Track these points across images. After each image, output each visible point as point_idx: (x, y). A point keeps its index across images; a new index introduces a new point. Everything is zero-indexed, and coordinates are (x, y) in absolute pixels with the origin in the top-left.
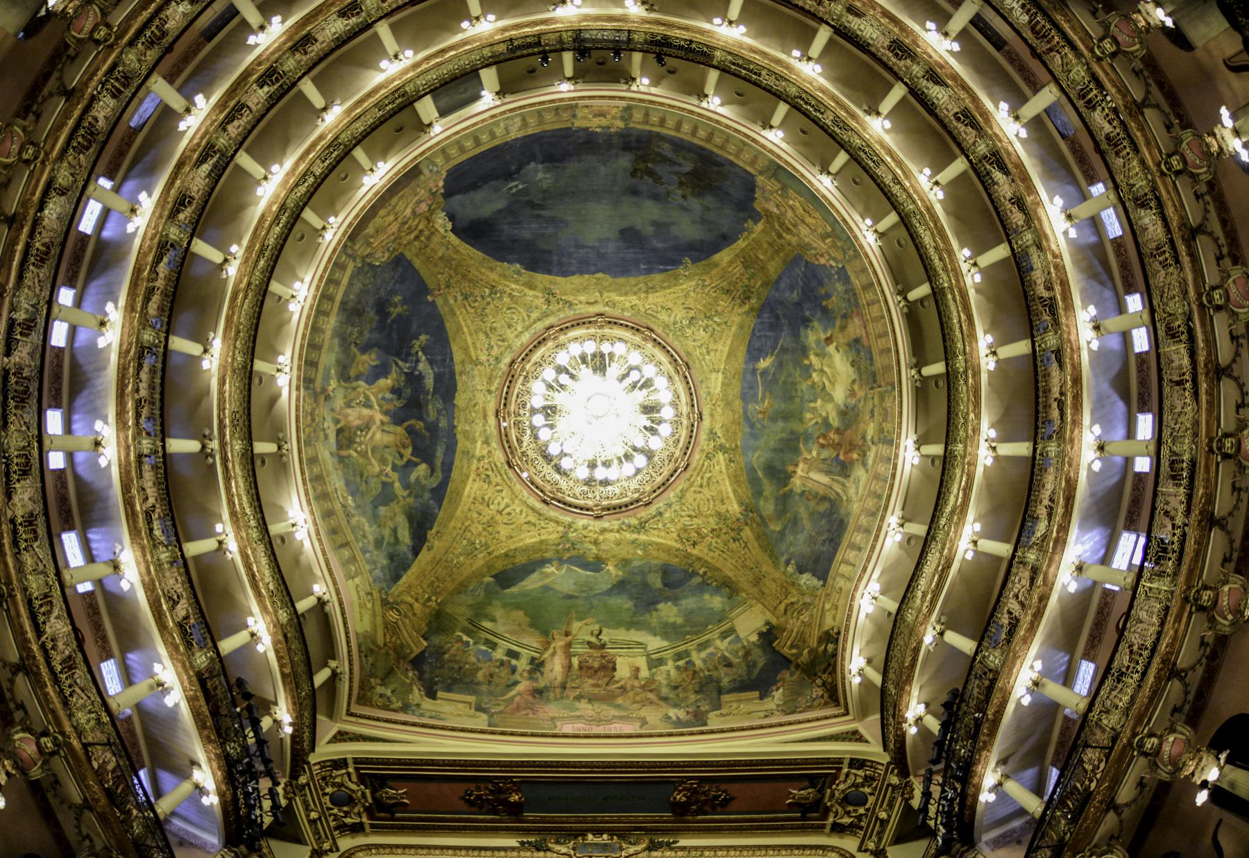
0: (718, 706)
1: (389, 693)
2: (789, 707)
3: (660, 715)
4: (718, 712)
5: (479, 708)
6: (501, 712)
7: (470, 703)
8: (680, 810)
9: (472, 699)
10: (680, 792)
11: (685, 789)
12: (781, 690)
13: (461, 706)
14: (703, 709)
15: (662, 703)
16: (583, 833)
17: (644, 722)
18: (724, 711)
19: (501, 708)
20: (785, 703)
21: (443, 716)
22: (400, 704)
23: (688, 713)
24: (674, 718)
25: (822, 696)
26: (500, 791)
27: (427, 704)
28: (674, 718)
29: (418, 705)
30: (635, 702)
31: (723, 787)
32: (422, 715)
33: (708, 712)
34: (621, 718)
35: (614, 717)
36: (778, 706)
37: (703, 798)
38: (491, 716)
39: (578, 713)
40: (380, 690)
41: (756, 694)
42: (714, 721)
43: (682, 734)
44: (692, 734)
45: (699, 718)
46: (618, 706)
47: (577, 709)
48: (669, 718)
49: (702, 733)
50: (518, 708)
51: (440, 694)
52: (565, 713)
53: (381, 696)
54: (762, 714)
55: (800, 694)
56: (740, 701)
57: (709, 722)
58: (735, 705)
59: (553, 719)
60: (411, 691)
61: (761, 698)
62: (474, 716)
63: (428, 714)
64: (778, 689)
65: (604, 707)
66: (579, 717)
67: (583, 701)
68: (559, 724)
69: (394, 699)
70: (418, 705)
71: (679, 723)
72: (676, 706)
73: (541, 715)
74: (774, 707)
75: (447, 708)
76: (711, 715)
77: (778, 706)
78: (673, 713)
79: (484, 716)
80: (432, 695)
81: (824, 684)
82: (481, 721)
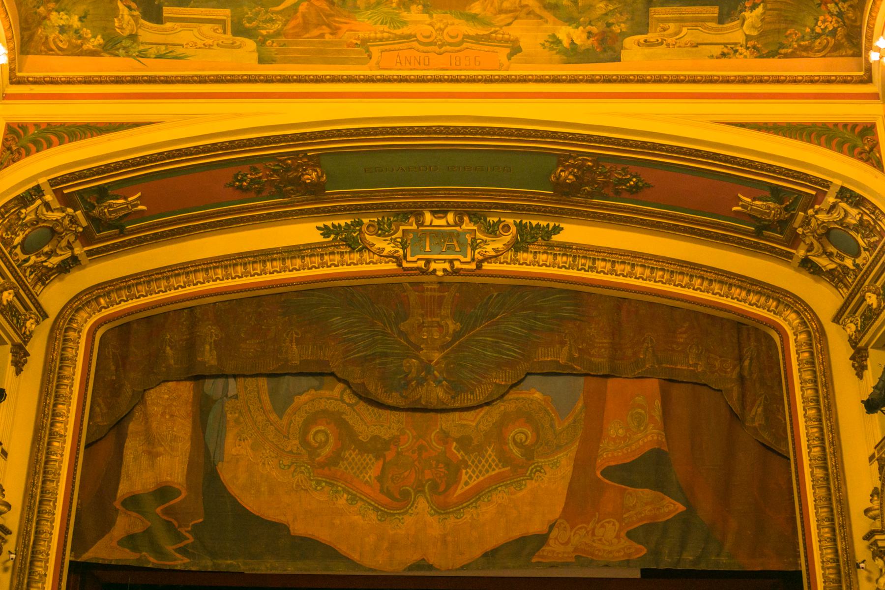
0: (642, 27)
1: (75, 21)
2: (768, 46)
3: (542, 37)
4: (641, 38)
5: (239, 30)
6: (278, 34)
7: (222, 22)
8: (564, 191)
9: (224, 13)
10: (567, 168)
11: (574, 166)
12: (760, 10)
13: (207, 28)
14: (616, 29)
15: (545, 14)
16: (417, 212)
17: (515, 50)
18: (652, 36)
19: (277, 26)
20: (762, 34)
21: (179, 51)
22: (99, 40)
23: (590, 34)
24: (566, 43)
25: (834, 33)
26: (288, 169)
27: (149, 32)
28: (566, 43)
29: (133, 37)
30: (501, 11)
31: (633, 169)
32: (142, 55)
33: (624, 35)
34: (477, 39)
35: (468, 37)
36: (748, 38)
37: (600, 179)
38: (261, 43)
39: (406, 30)
40: (57, 19)
41: (714, 11)
42: (635, 56)
43: (574, 80)
44: (591, 80)
45: (607, 47)
46: (474, 18)
47: (405, 23)
48: (558, 42)
49: (608, 80)
50: (306, 26)
51: (167, 11)
52: (383, 30)
53: (63, 29)
54: (717, 50)
55: (793, 22)
56: (681, 20)
57: (624, 54)
58: (672, 27)
59: (364, 42)
60: (115, 12)
61: (721, 20)
62: (232, 46)
63: (153, 51)
64: (754, 7)
65: (450, 19)
66: (408, 37)
67: (414, 7)
68: (375, 51)
69: (87, 32)
70: (133, 37)
71: (574, 54)
72: (571, 20)
73: (346, 36)
74: (741, 39)
75: (184, 35)
76: (629, 41)
77: (748, 38)
78: (565, 33)
79: (250, 44)
80: (154, 14)
81: (840, 14)
82: (244, 56)
